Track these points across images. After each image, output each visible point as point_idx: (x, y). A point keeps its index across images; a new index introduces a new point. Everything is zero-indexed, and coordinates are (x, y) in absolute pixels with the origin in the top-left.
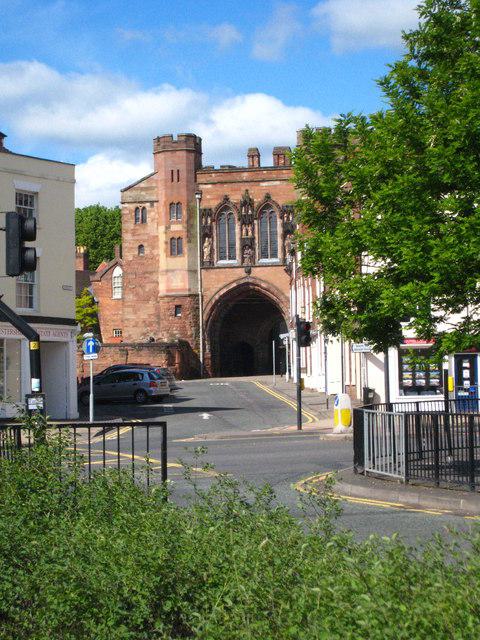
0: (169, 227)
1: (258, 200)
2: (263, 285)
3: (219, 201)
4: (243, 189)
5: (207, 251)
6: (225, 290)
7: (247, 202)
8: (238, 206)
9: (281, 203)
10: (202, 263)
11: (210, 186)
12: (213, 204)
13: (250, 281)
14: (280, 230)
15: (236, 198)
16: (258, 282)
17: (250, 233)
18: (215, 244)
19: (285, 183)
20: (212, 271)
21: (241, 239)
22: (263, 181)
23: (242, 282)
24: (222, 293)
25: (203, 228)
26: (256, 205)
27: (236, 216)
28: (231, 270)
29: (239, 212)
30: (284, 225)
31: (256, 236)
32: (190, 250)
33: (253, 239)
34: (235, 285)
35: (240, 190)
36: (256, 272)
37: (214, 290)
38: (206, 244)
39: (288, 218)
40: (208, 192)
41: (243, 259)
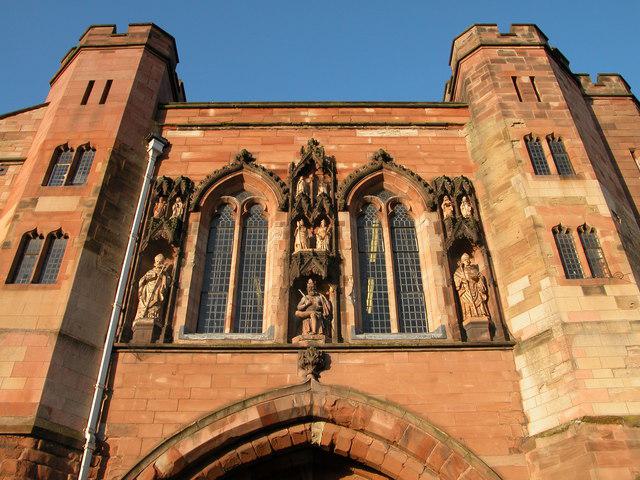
0: (35, 202)
1: (346, 168)
2: (381, 422)
3: (219, 167)
4: (303, 139)
5: (150, 291)
6: (206, 436)
7: (313, 165)
8: (285, 179)
9: (429, 174)
10: (126, 333)
11: (196, 133)
12: (200, 172)
13: (321, 401)
14: (427, 240)
15: (279, 153)
16: (353, 406)
17: (321, 245)
18: (187, 275)
19: (431, 134)
20: (158, 359)
21: (290, 257)
22: (365, 125)
23: (284, 405)
24: (187, 446)
25: (149, 222)
26: (342, 178)
27: (270, 202)
28: (239, 358)
29: (287, 191)
30: (441, 227)
31: (347, 254)
32: (84, 271)
33: (334, 262)
34: (252, 415)
35: (291, 142)
36: (347, 368)
37: (155, 434)
38: (151, 273)
39: (456, 210)
40: (189, 145)
41: (294, 326)
